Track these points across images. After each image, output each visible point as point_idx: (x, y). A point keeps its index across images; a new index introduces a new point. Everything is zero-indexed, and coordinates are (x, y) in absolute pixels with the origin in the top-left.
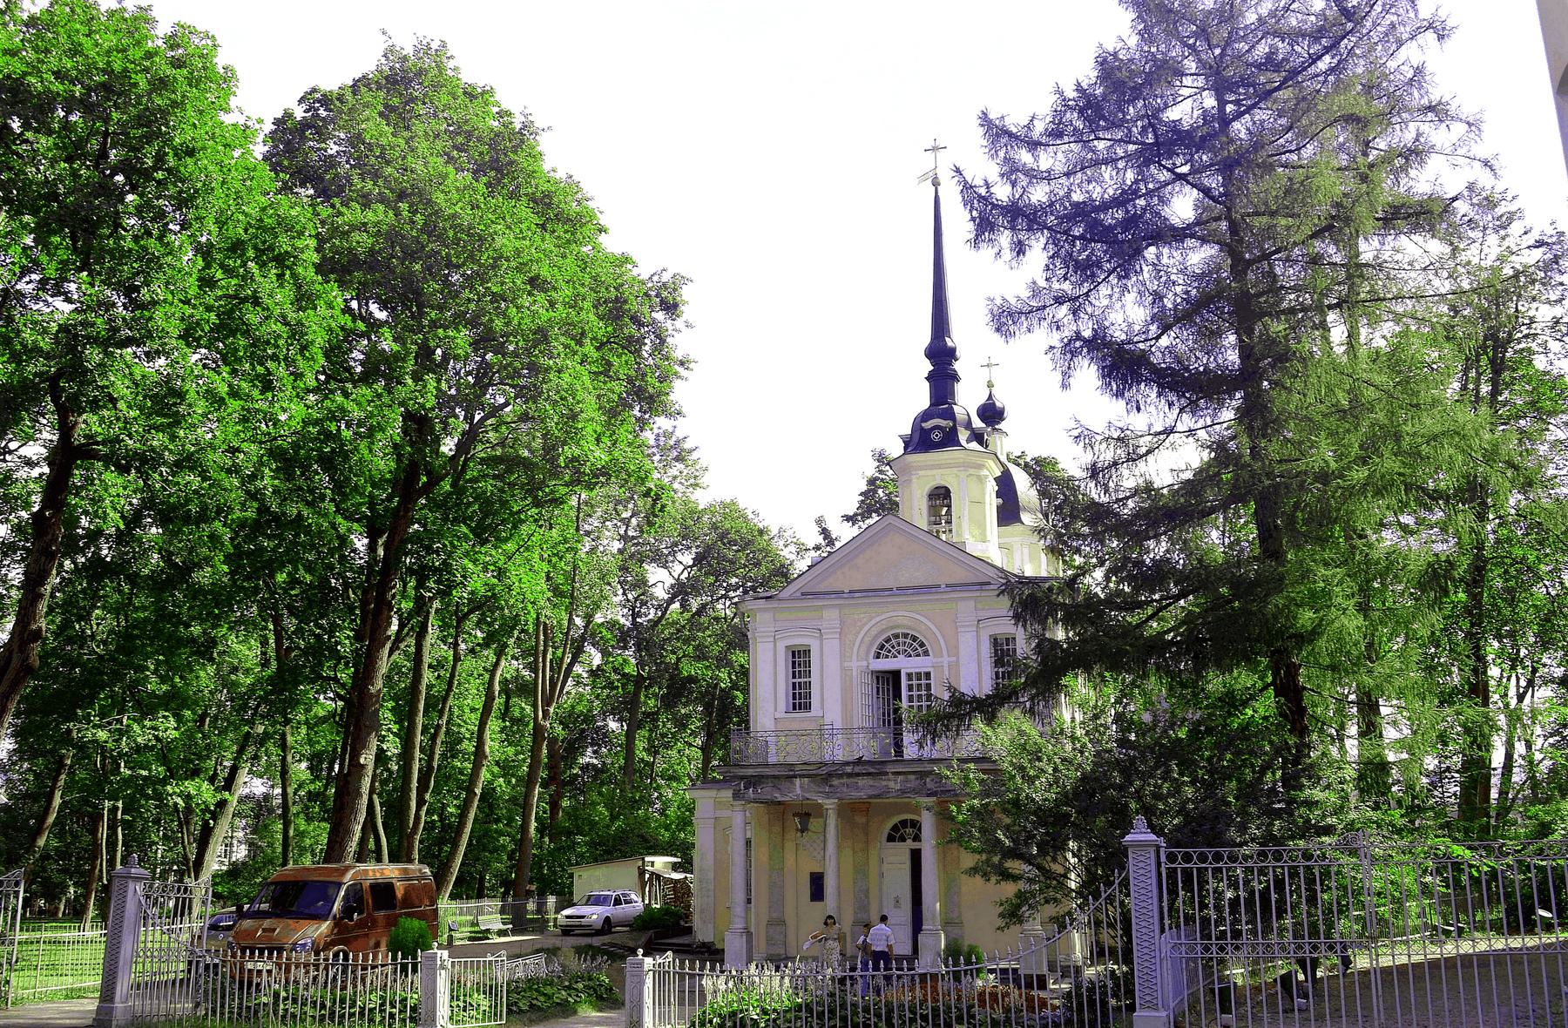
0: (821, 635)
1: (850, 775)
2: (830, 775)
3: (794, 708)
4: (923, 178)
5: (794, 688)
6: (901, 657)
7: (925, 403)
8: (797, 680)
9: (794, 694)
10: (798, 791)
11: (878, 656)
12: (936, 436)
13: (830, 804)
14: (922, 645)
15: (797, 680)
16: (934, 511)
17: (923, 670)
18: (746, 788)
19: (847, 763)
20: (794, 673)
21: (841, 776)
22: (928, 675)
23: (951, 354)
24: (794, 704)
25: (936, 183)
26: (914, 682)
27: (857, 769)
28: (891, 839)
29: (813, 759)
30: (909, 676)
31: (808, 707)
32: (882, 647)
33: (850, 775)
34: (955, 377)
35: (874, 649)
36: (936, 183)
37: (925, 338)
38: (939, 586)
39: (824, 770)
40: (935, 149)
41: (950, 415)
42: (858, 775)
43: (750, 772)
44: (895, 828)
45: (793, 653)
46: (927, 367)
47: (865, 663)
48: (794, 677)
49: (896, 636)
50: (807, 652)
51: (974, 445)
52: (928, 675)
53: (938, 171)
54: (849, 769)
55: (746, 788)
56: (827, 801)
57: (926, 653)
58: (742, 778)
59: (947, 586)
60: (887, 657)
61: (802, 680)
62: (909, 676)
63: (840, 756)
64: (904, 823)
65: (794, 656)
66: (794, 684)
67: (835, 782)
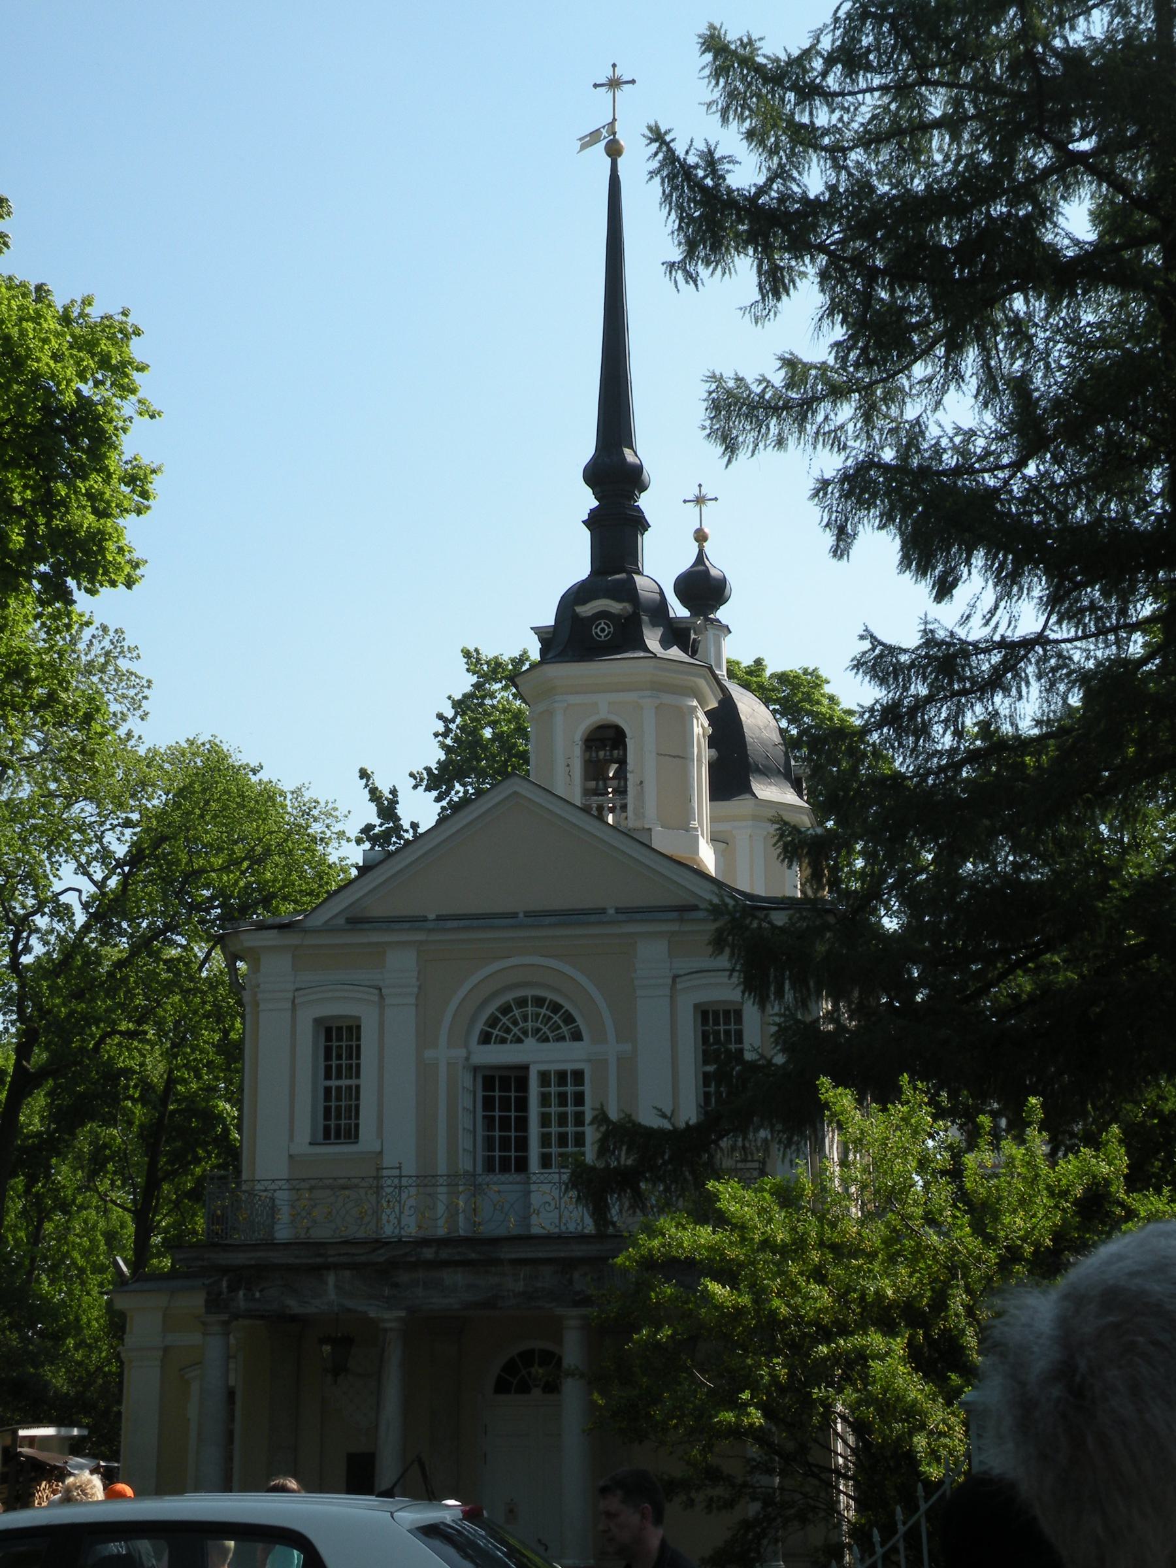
0: (381, 996)
3: (327, 1135)
4: (594, 137)
5: (327, 1097)
6: (530, 1042)
7: (579, 567)
8: (333, 1083)
9: (327, 1110)
10: (332, 1295)
11: (486, 1039)
12: (603, 632)
13: (390, 1318)
14: (569, 1019)
15: (333, 1083)
16: (594, 771)
17: (569, 1067)
18: (232, 1289)
19: (425, 1242)
20: (328, 1069)
22: (578, 1076)
23: (634, 479)
24: (327, 1130)
25: (614, 151)
26: (553, 1089)
27: (445, 1254)
28: (501, 1387)
29: (361, 1234)
30: (544, 1077)
31: (351, 1134)
32: (493, 1022)
34: (640, 524)
35: (480, 1025)
36: (614, 151)
37: (585, 447)
38: (603, 911)
40: (614, 84)
41: (628, 592)
42: (446, 1264)
44: (510, 1367)
45: (328, 1031)
46: (588, 501)
47: (463, 1053)
48: (328, 1077)
49: (522, 1002)
50: (353, 1030)
51: (675, 653)
52: (578, 1076)
53: (618, 127)
54: (428, 1253)
55: (232, 1289)
56: (387, 1315)
57: (577, 1036)
59: (618, 911)
60: (503, 1041)
61: (344, 1082)
62: (544, 1077)
63: (411, 1228)
64: (527, 1357)
65: (328, 1038)
66: (328, 1090)
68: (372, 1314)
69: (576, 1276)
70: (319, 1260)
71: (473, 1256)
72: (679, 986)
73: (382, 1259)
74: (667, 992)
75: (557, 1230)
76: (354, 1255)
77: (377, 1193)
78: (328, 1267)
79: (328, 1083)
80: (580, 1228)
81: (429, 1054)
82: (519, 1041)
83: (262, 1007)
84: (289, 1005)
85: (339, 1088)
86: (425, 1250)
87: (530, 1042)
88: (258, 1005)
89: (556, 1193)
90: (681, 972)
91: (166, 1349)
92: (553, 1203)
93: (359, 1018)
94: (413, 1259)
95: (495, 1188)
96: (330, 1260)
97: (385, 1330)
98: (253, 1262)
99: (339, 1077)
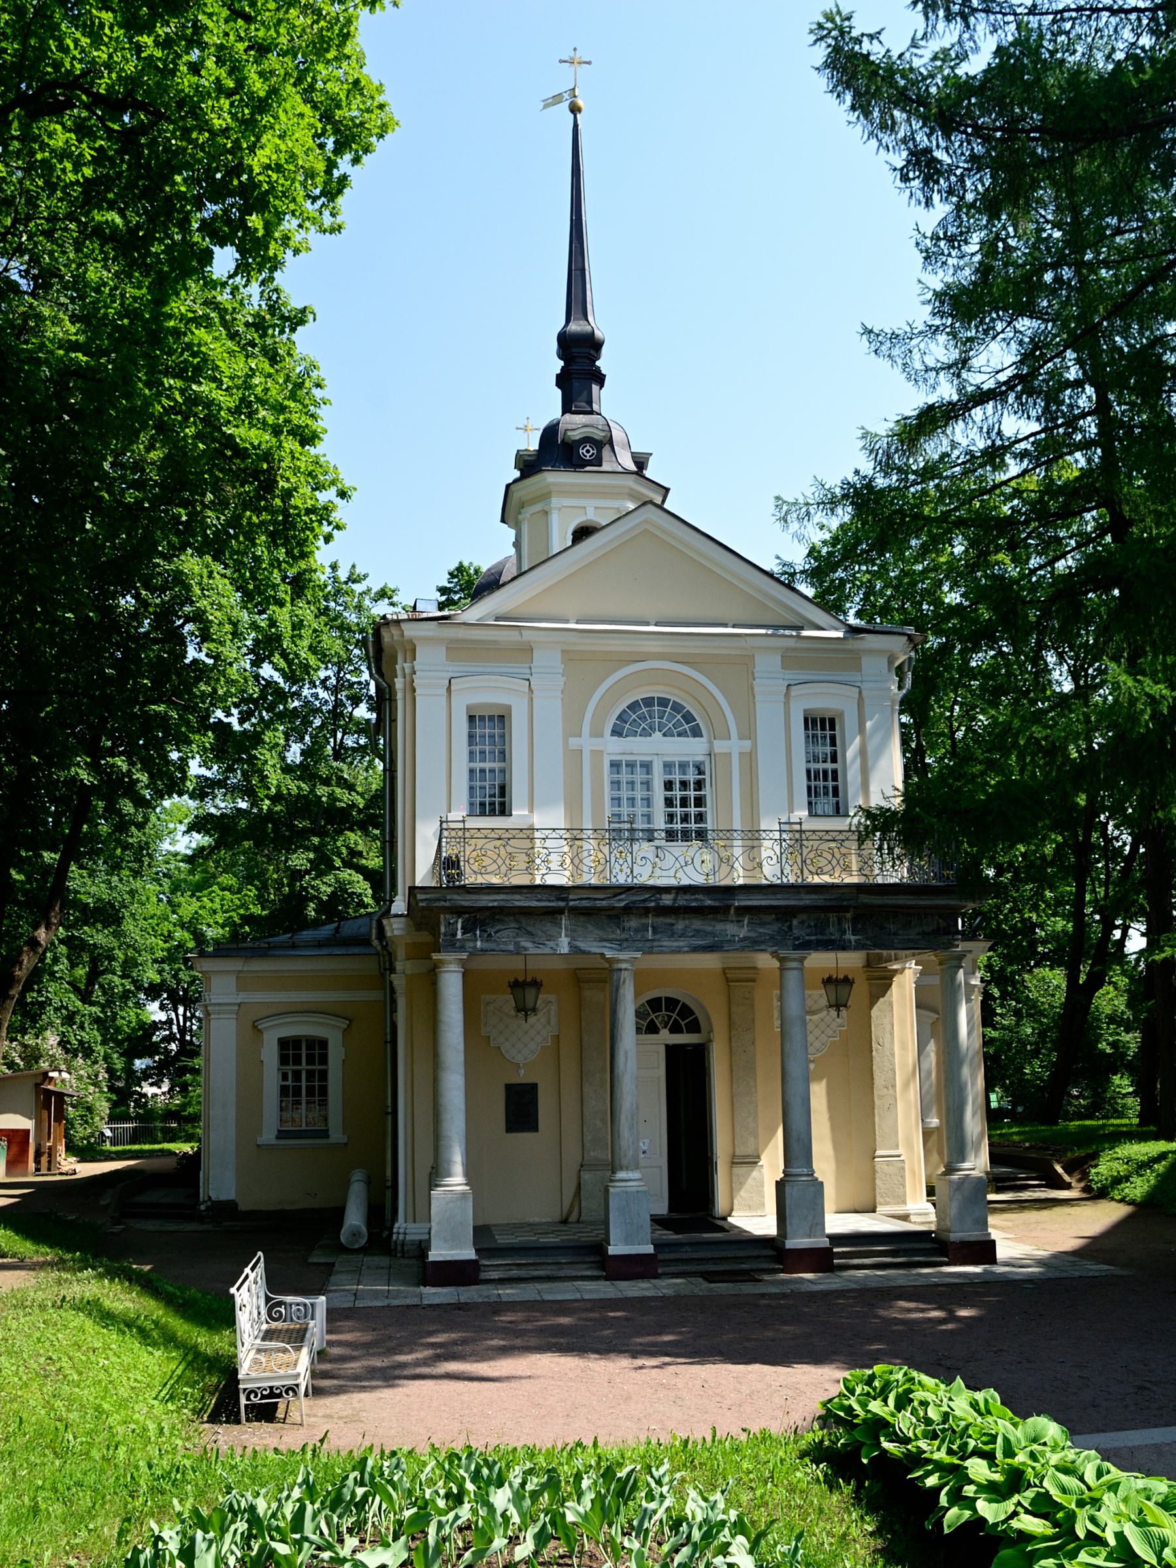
1: (662, 911)
2: (627, 910)
6: (658, 735)
9: (471, 788)
11: (617, 732)
15: (478, 765)
19: (667, 890)
21: (646, 911)
27: (681, 902)
30: (668, 766)
33: (662, 911)
34: (600, 379)
35: (612, 720)
39: (620, 902)
43: (486, 900)
50: (501, 719)
54: (667, 900)
56: (623, 956)
57: (696, 733)
58: (458, 911)
61: (487, 765)
62: (668, 766)
66: (471, 771)
67: (634, 923)
68: (609, 954)
69: (795, 922)
70: (562, 904)
71: (709, 903)
72: (793, 694)
73: (622, 904)
74: (782, 698)
75: (779, 882)
76: (596, 899)
77: (610, 844)
78: (560, 911)
79: (473, 765)
80: (800, 880)
81: (574, 742)
82: (646, 733)
83: (418, 692)
84: (444, 691)
85: (482, 771)
86: (664, 896)
87: (658, 735)
88: (414, 690)
89: (777, 849)
90: (792, 682)
91: (239, 1005)
92: (775, 858)
93: (509, 708)
94: (653, 904)
95: (722, 843)
96: (571, 903)
97: (621, 970)
98: (496, 904)
99: (483, 760)
